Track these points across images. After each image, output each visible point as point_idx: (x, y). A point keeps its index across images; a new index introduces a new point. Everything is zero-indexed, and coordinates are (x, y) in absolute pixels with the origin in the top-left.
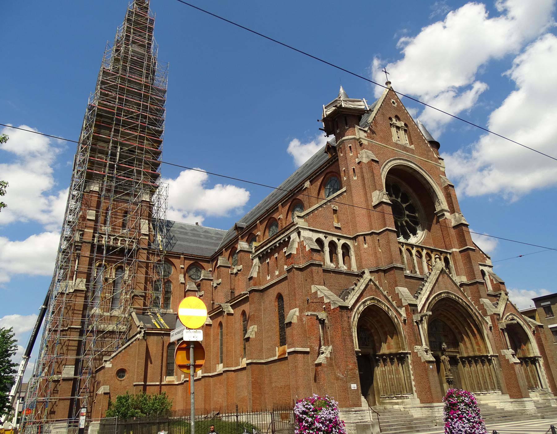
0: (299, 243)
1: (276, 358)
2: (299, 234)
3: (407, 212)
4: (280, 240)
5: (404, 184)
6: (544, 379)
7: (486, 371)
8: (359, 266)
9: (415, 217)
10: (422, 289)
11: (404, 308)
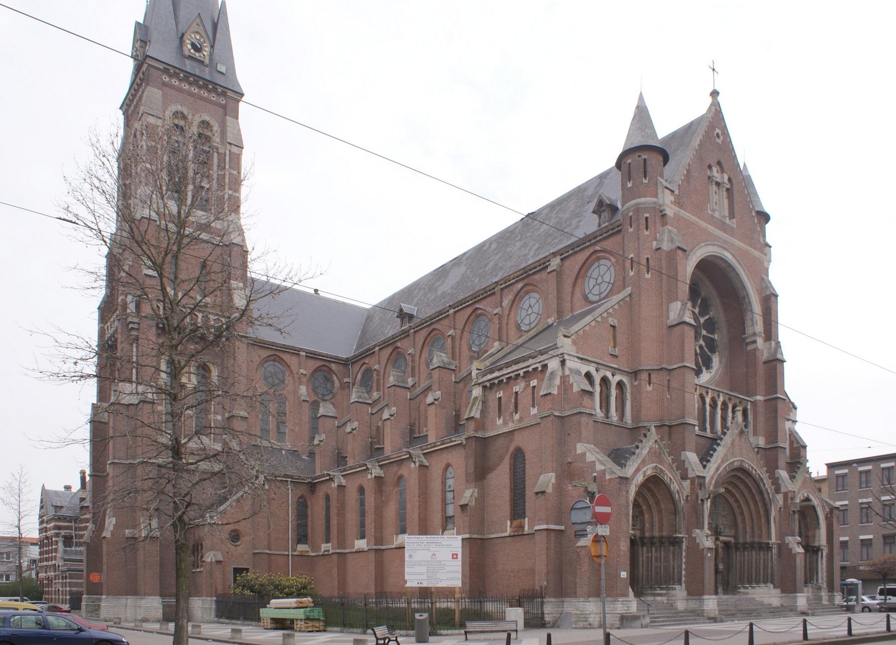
0: (561, 377)
1: (507, 534)
2: (563, 362)
3: (704, 332)
4: (528, 366)
5: (707, 283)
6: (822, 573)
7: (762, 562)
8: (636, 417)
9: (713, 340)
10: (712, 455)
11: (689, 481)
